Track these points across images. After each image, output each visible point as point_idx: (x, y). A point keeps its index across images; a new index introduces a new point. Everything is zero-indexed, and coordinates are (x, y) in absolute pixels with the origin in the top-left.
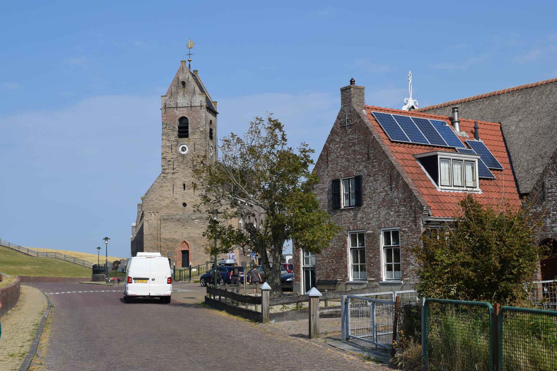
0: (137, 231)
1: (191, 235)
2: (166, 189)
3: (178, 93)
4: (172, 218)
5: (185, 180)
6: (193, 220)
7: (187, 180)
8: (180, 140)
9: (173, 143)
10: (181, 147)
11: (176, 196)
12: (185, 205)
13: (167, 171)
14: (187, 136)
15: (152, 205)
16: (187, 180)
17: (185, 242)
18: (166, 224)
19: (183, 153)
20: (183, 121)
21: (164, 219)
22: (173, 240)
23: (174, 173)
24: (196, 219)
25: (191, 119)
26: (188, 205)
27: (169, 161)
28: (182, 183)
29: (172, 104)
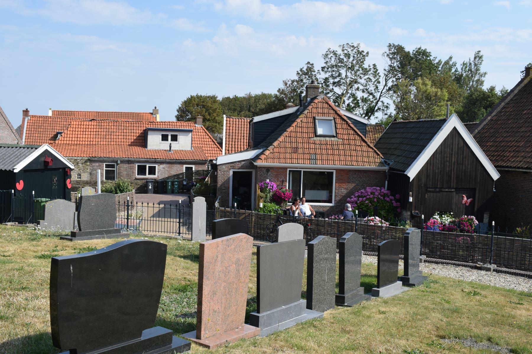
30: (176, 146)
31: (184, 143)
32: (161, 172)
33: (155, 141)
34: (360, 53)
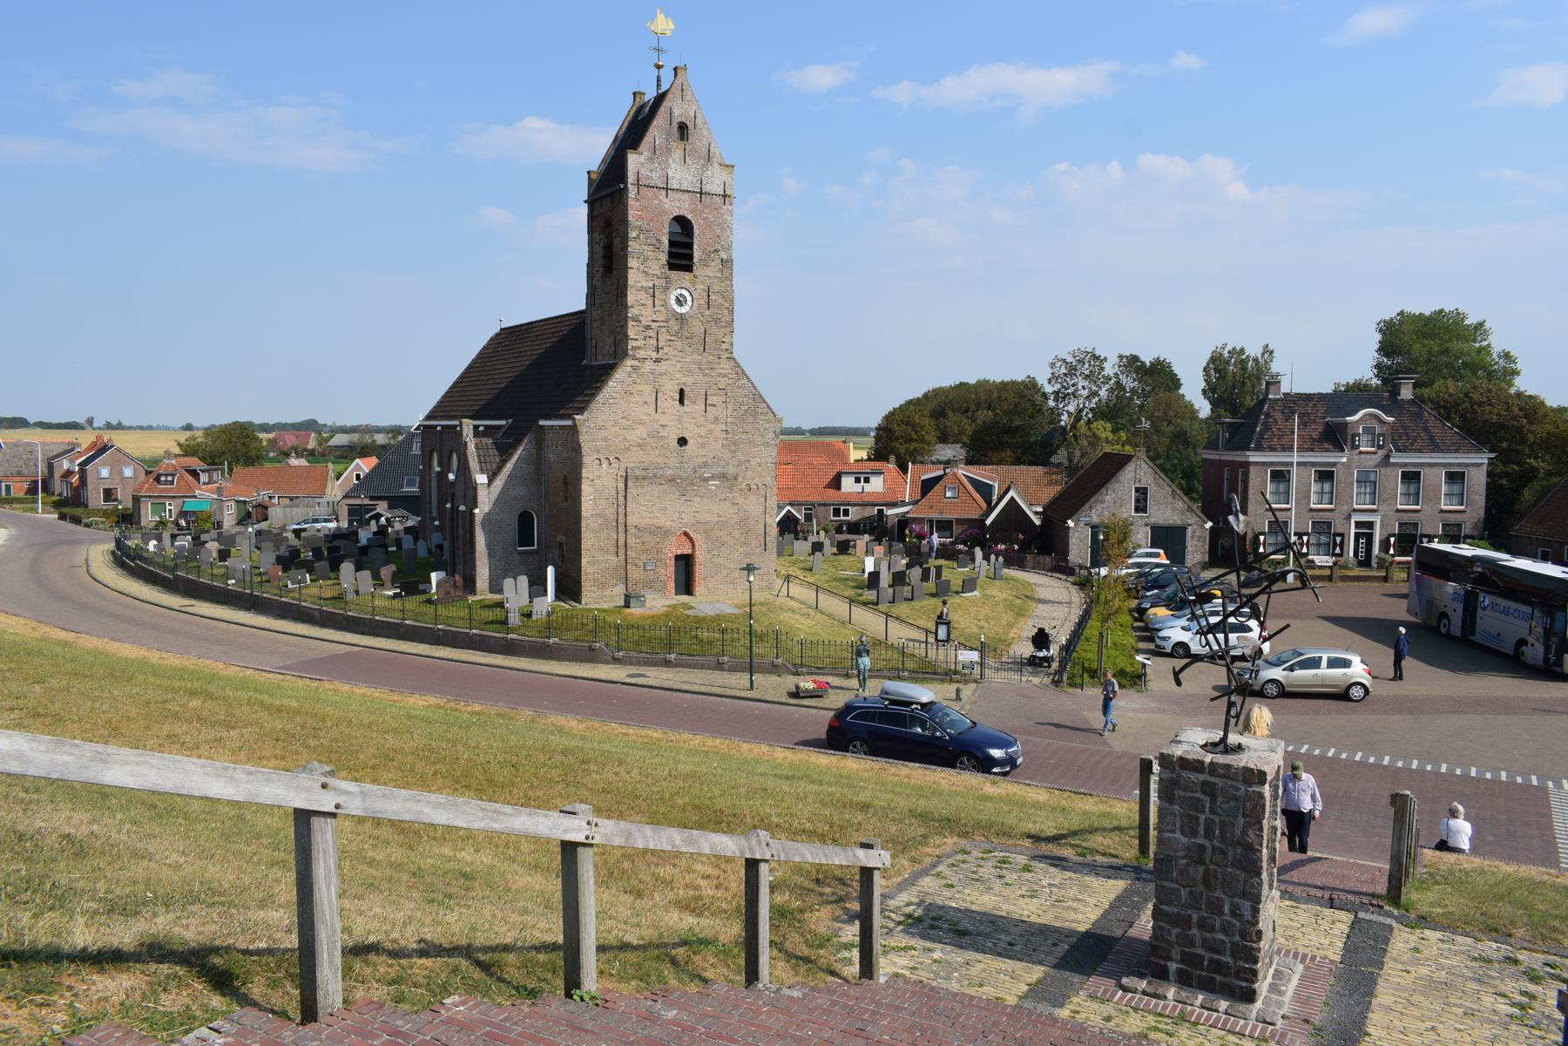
0: (494, 496)
1: (704, 517)
2: (638, 398)
3: (669, 150)
4: (655, 476)
6: (706, 480)
7: (689, 380)
8: (674, 274)
9: (659, 282)
11: (664, 420)
12: (682, 441)
13: (641, 354)
14: (689, 268)
15: (605, 440)
16: (689, 380)
17: (686, 534)
18: (641, 491)
19: (679, 310)
20: (683, 223)
21: (637, 478)
22: (661, 532)
23: (657, 361)
24: (713, 477)
26: (690, 442)
27: (648, 327)
28: (677, 389)
30: (868, 488)
31: (876, 485)
32: (854, 514)
33: (848, 484)
34: (1096, 358)
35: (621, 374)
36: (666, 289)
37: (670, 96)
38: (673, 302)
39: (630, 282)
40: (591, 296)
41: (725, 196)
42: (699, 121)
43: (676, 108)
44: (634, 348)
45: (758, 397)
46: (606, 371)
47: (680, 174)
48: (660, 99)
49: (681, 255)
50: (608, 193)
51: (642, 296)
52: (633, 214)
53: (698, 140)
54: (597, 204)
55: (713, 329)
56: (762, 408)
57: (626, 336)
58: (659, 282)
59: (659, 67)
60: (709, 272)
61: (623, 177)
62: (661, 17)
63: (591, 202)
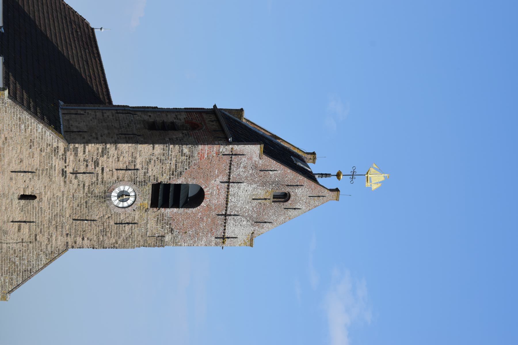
2: (26, 153)
3: (264, 184)
5: (45, 199)
8: (148, 189)
9: (141, 173)
10: (130, 190)
13: (70, 157)
14: (154, 204)
16: (44, 205)
19: (114, 194)
23: (64, 173)
25: (195, 215)
27: (96, 164)
28: (36, 193)
29: (238, 172)
35: (50, 136)
36: (134, 182)
37: (313, 184)
38: (122, 188)
39: (140, 147)
40: (125, 110)
41: (224, 238)
42: (291, 213)
43: (303, 191)
44: (76, 150)
45: (28, 274)
46: (52, 122)
47: (243, 195)
48: (311, 176)
49: (167, 196)
50: (225, 127)
51: (127, 158)
52: (205, 150)
53: (274, 211)
54: (213, 117)
55: (95, 228)
56: (17, 279)
57: (88, 142)
58: (141, 173)
59: (338, 175)
60: (152, 224)
61: (238, 141)
62: (381, 177)
63: (214, 111)
